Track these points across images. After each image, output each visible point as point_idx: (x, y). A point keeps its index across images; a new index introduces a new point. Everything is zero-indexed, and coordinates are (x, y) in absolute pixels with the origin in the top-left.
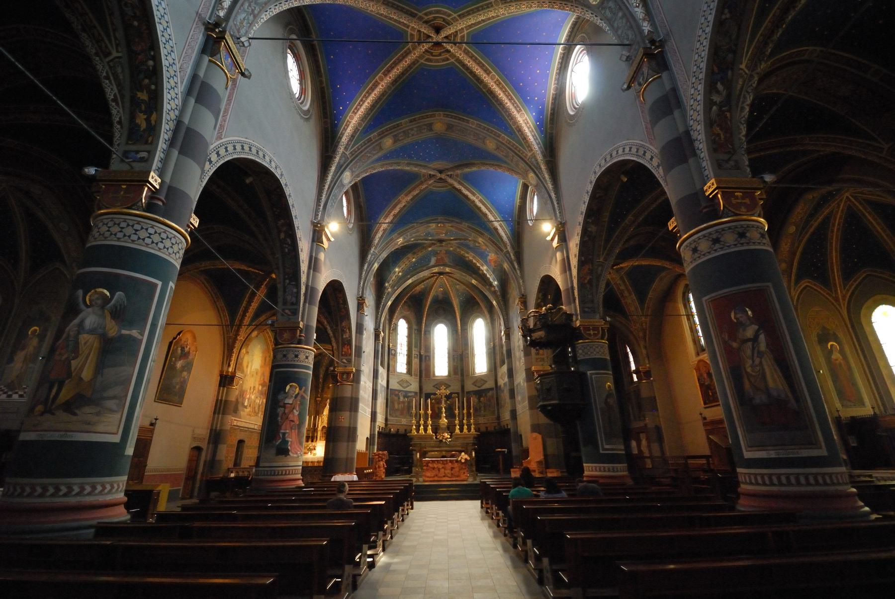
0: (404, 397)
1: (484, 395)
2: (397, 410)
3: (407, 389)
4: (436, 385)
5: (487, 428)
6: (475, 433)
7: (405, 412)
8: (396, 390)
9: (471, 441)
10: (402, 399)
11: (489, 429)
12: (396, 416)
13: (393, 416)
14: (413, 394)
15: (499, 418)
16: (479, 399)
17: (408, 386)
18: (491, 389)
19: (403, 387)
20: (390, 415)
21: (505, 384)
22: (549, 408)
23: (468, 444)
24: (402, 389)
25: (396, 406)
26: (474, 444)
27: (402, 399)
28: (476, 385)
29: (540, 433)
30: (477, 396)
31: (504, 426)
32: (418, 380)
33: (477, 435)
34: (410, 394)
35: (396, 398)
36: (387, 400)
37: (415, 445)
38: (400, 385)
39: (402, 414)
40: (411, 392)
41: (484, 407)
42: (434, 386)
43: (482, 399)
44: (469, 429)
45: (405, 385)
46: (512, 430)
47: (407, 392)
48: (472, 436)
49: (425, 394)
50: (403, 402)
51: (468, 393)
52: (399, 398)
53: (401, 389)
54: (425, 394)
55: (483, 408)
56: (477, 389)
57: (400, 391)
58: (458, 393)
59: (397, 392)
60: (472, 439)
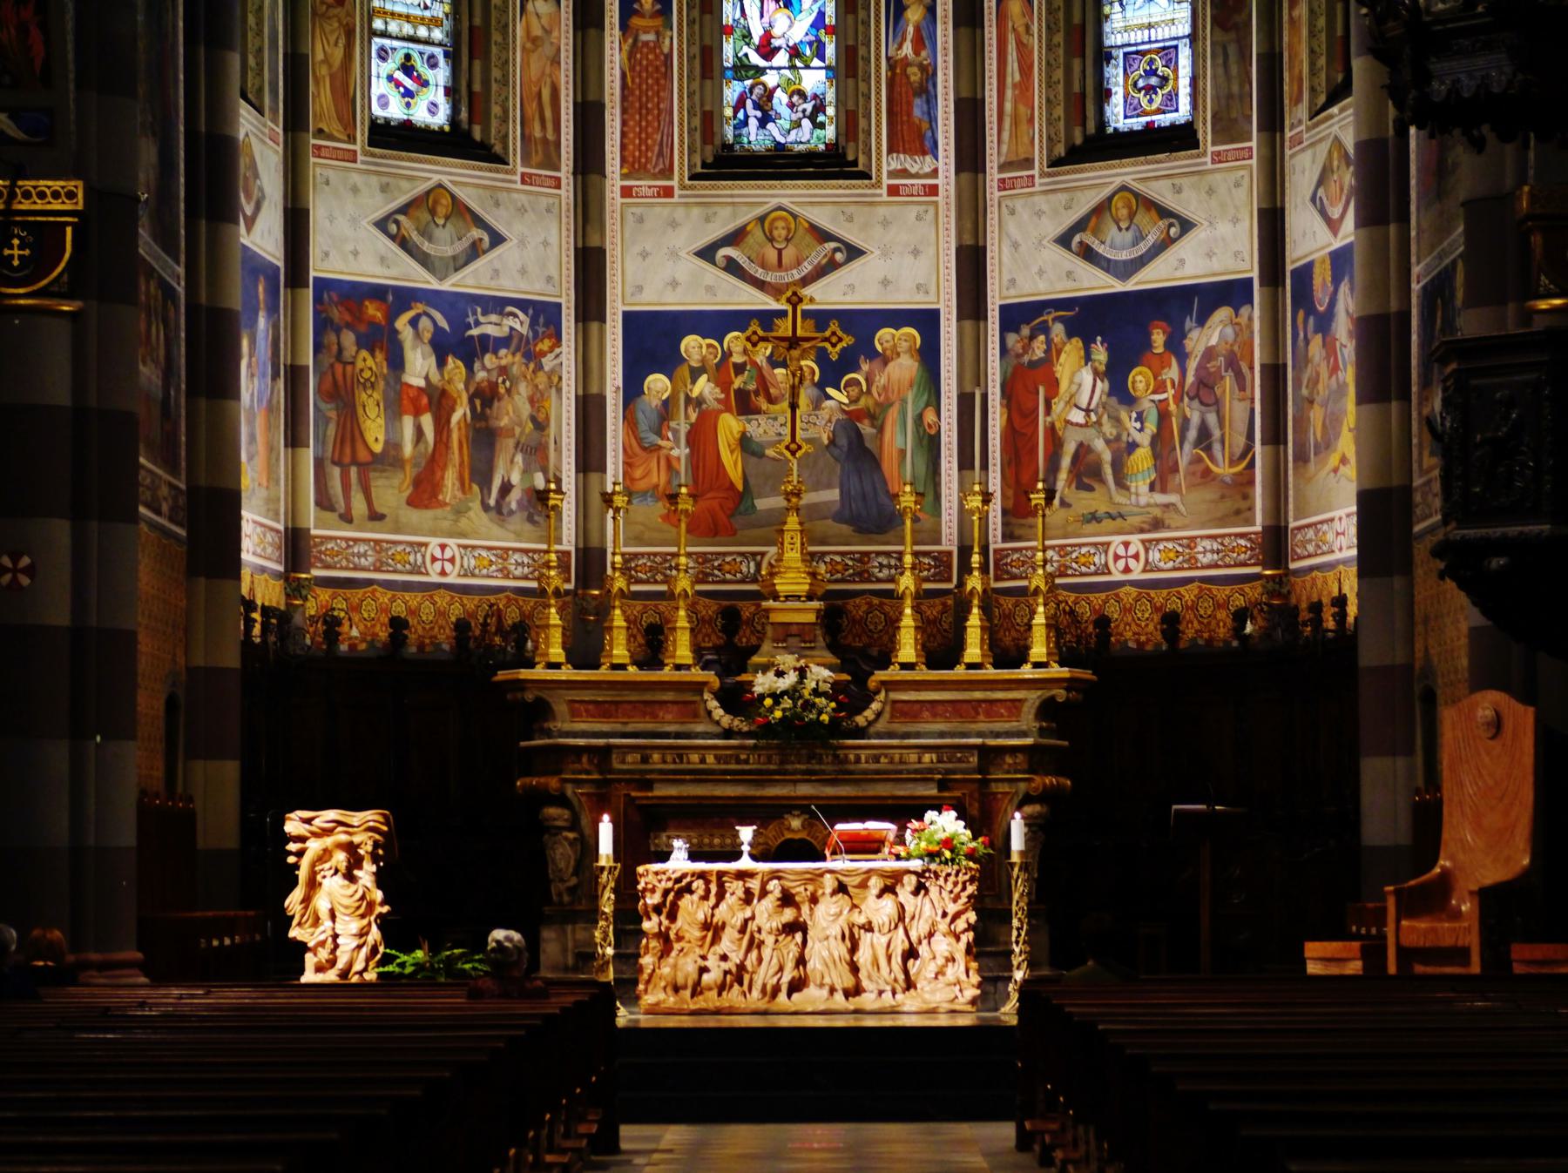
0: (442, 348)
1: (1158, 338)
2: (389, 459)
3: (469, 281)
4: (736, 237)
5: (1171, 621)
6: (1057, 671)
7: (450, 478)
8: (377, 292)
9: (1023, 730)
10: (419, 366)
11: (1189, 632)
12: (375, 517)
13: (347, 518)
14: (519, 323)
15: (1275, 543)
16: (1116, 377)
17: (474, 252)
18: (1232, 293)
19: (424, 260)
20: (324, 502)
21: (1340, 260)
22: (1498, 562)
23: (989, 756)
24: (421, 279)
25: (375, 431)
26: (1036, 758)
27: (419, 366)
28: (1088, 254)
29: (1526, 698)
30: (1101, 354)
31: (1317, 607)
32: (567, 192)
33: (1070, 684)
34: (491, 326)
35: (369, 363)
36: (295, 377)
37: (559, 757)
38: (404, 243)
39: (424, 492)
40: (497, 305)
41: (1161, 443)
42: (707, 253)
43: (1139, 379)
44: (1008, 652)
45: (445, 243)
46: (1369, 655)
47: (458, 306)
48: (1033, 697)
49: (628, 317)
50: (437, 400)
51: (1014, 316)
52: (397, 362)
53: (406, 272)
54: (632, 321)
55: (1142, 459)
56: (1096, 282)
57: (403, 298)
58: (927, 321)
59: (373, 311)
60: (1028, 720)
